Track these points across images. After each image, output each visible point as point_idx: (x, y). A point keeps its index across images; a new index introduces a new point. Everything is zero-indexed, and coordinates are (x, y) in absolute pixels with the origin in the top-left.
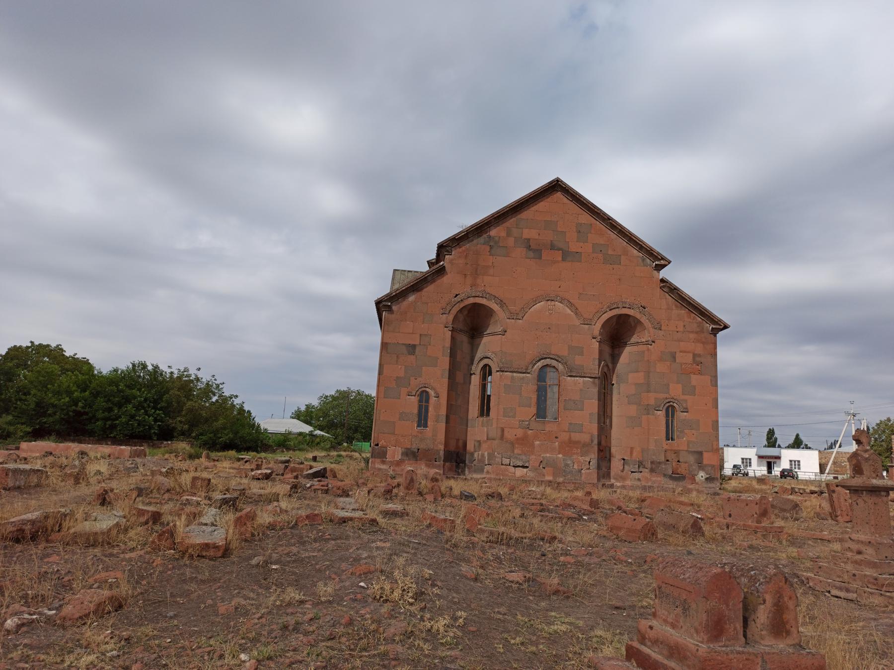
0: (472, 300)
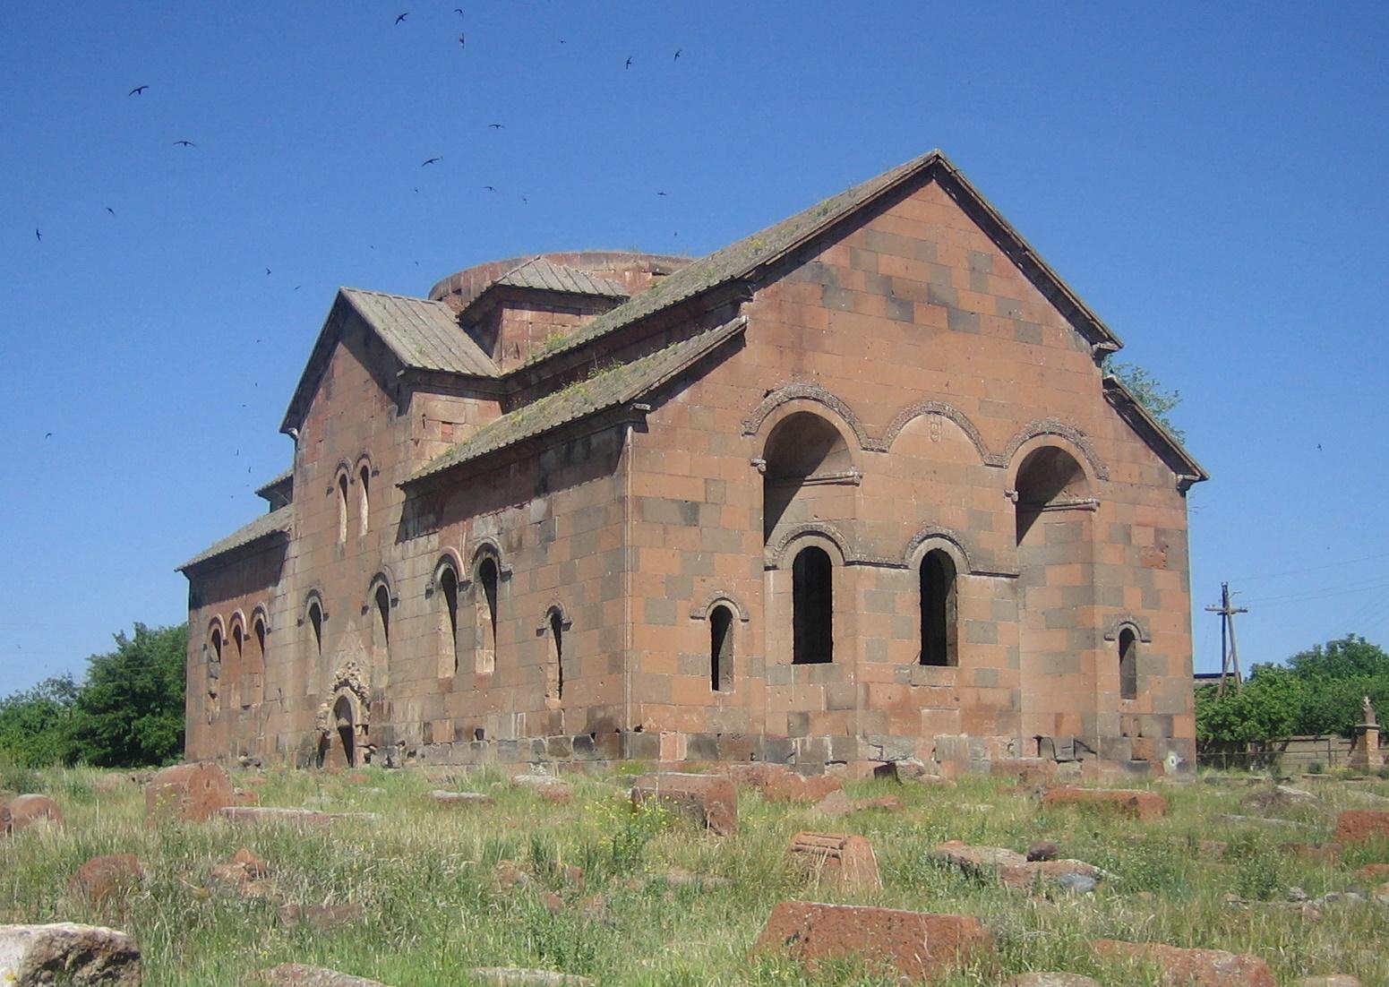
0: (796, 406)
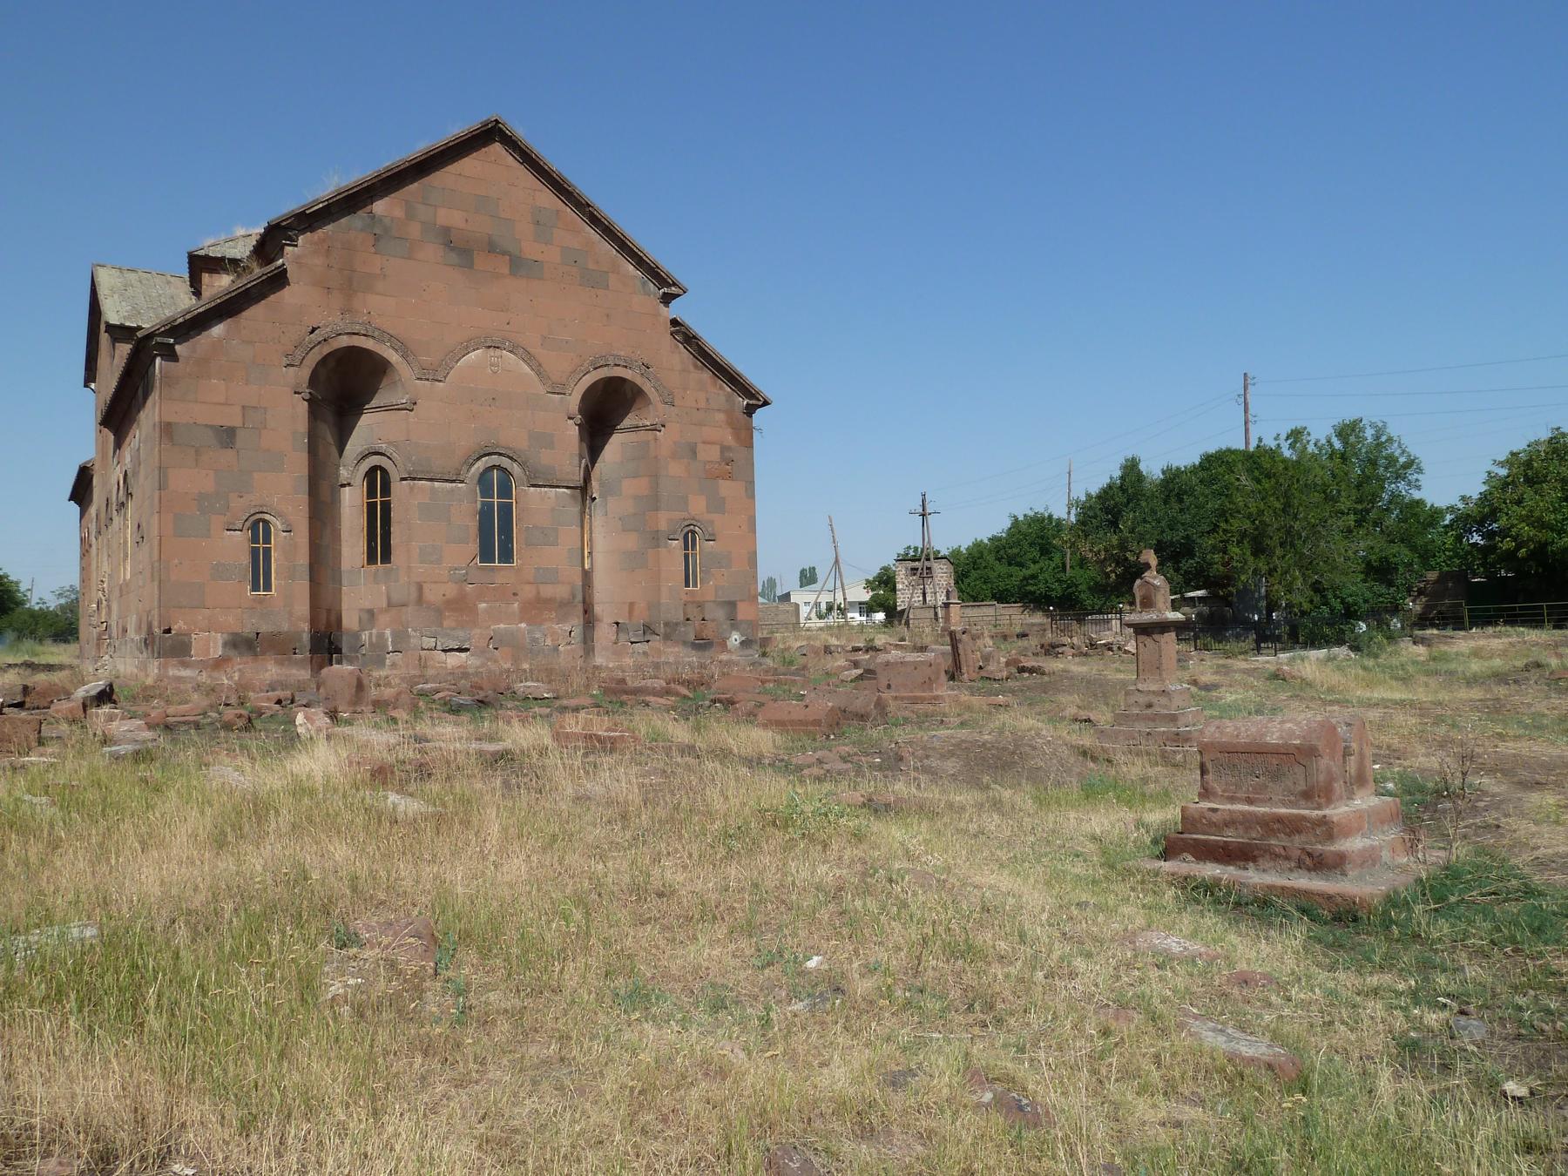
0: (344, 341)
